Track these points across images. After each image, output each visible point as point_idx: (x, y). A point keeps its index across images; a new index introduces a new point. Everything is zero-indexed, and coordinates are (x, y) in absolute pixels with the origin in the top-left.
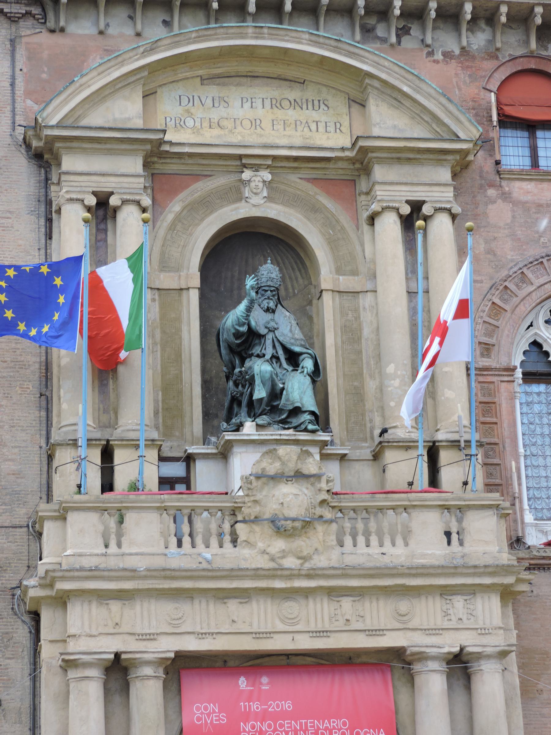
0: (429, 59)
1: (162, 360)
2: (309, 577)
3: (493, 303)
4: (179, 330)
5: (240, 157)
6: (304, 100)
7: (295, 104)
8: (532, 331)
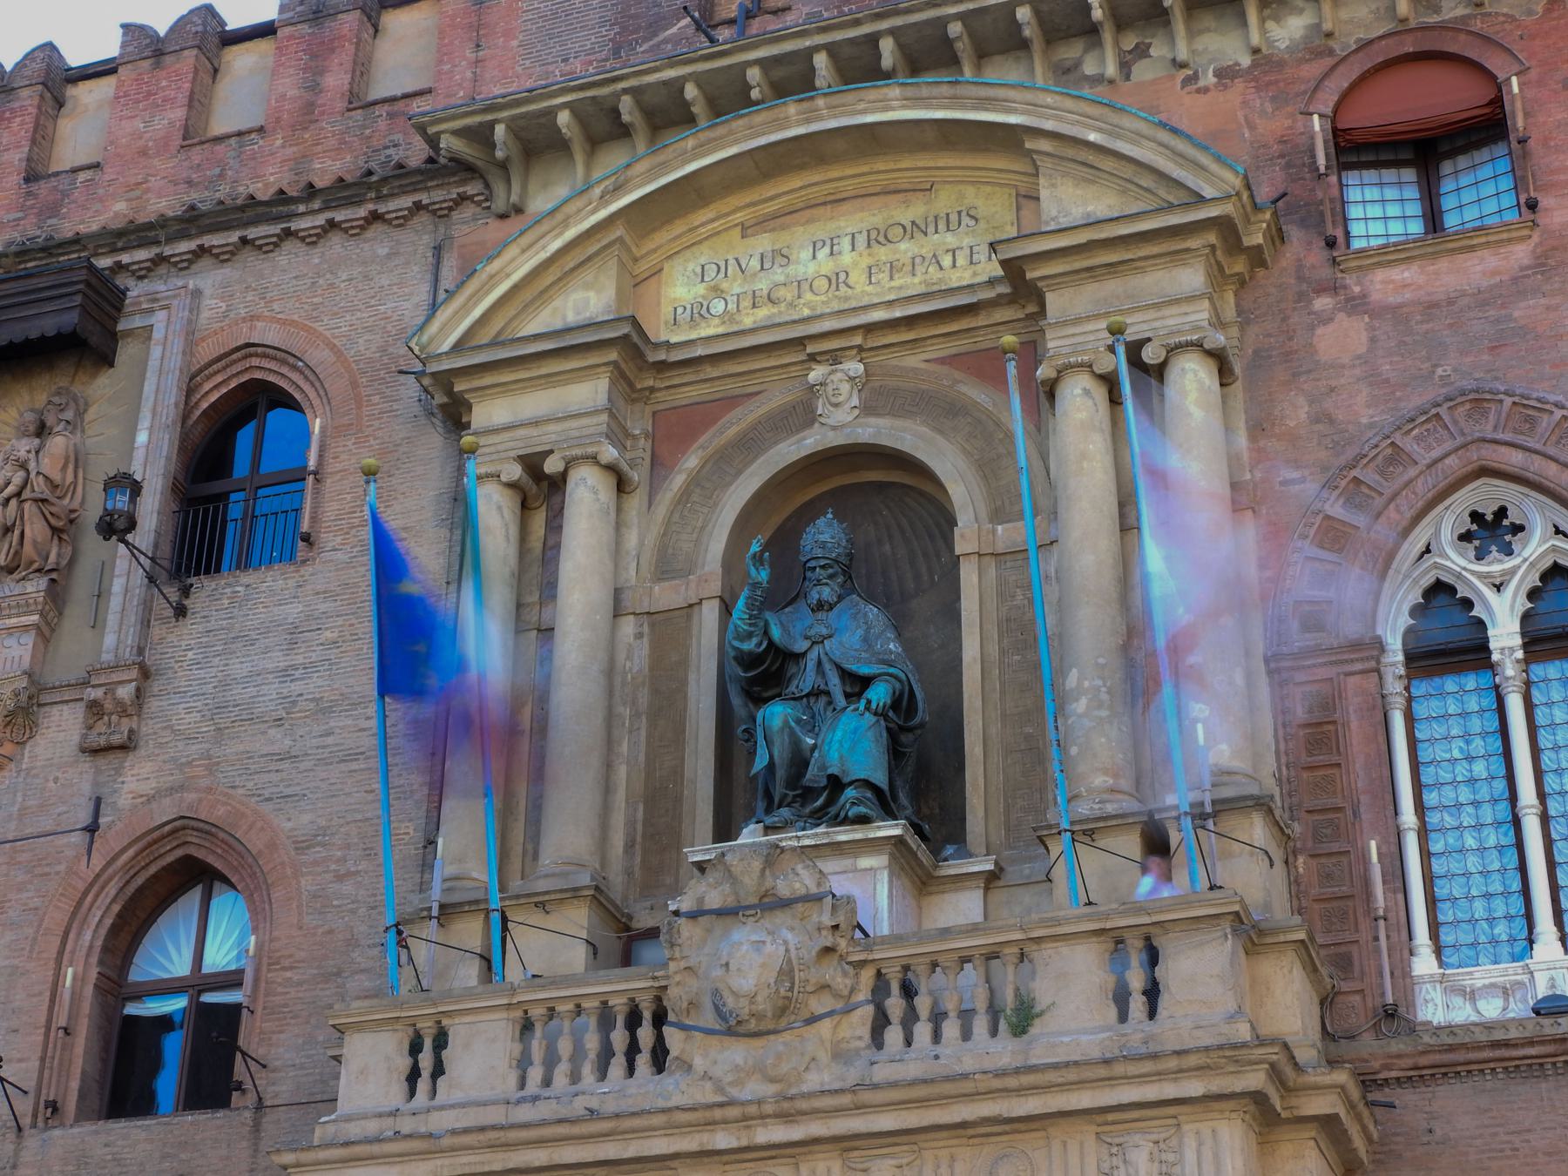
0: (1188, 89)
1: (648, 744)
2: (786, 1117)
3: (1328, 517)
4: (684, 682)
5: (800, 342)
6: (931, 219)
7: (915, 229)
8: (1429, 560)
